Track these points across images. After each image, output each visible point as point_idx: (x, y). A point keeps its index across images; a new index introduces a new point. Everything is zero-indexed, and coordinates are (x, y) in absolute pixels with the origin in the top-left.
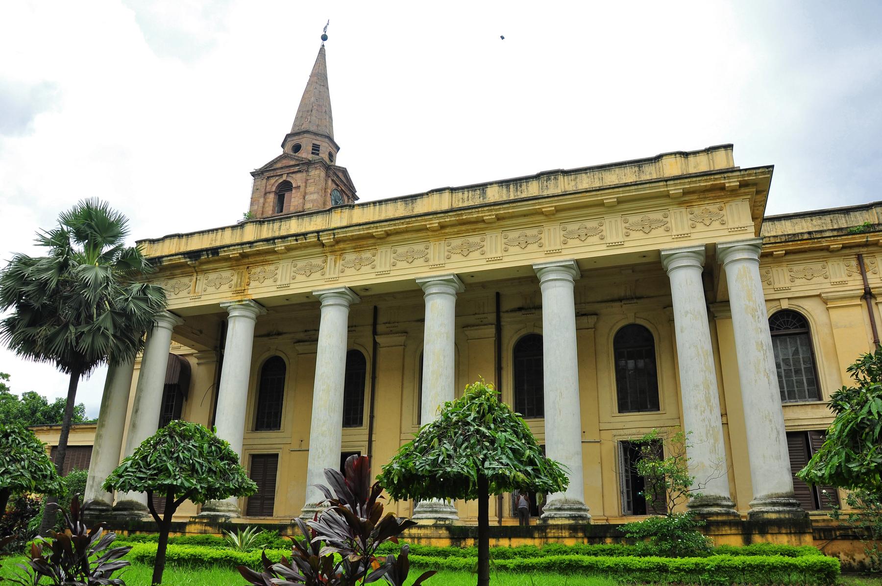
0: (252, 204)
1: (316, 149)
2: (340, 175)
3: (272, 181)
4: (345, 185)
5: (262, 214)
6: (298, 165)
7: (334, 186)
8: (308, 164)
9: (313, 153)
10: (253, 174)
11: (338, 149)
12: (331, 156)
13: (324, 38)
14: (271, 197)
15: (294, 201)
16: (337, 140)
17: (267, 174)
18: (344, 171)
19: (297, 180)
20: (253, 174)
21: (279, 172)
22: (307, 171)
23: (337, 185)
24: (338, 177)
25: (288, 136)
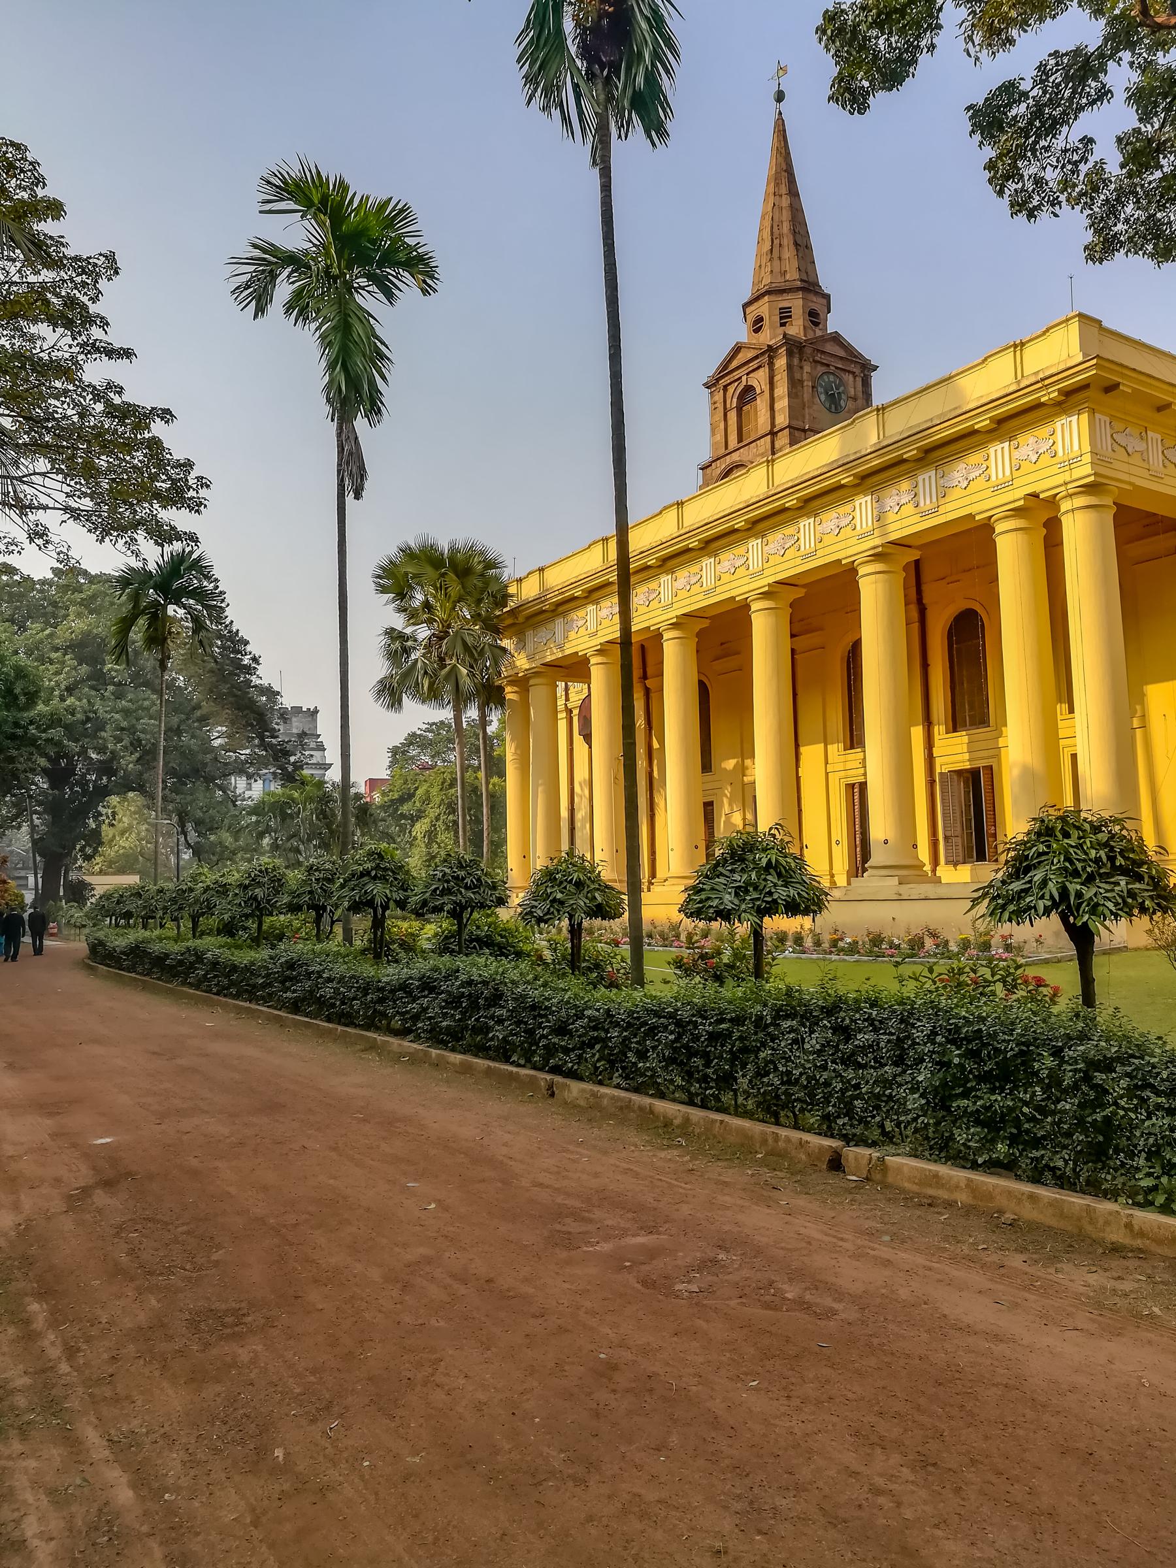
0: (713, 432)
1: (785, 316)
2: (830, 348)
3: (731, 389)
4: (841, 358)
5: (726, 448)
6: (756, 357)
7: (821, 369)
8: (771, 351)
9: (783, 325)
10: (708, 386)
11: (827, 297)
12: (815, 318)
13: (780, 97)
14: (733, 416)
15: (760, 417)
16: (826, 282)
17: (722, 382)
18: (836, 338)
19: (759, 380)
20: (708, 386)
21: (736, 375)
22: (771, 364)
23: (828, 365)
24: (823, 352)
25: (745, 306)
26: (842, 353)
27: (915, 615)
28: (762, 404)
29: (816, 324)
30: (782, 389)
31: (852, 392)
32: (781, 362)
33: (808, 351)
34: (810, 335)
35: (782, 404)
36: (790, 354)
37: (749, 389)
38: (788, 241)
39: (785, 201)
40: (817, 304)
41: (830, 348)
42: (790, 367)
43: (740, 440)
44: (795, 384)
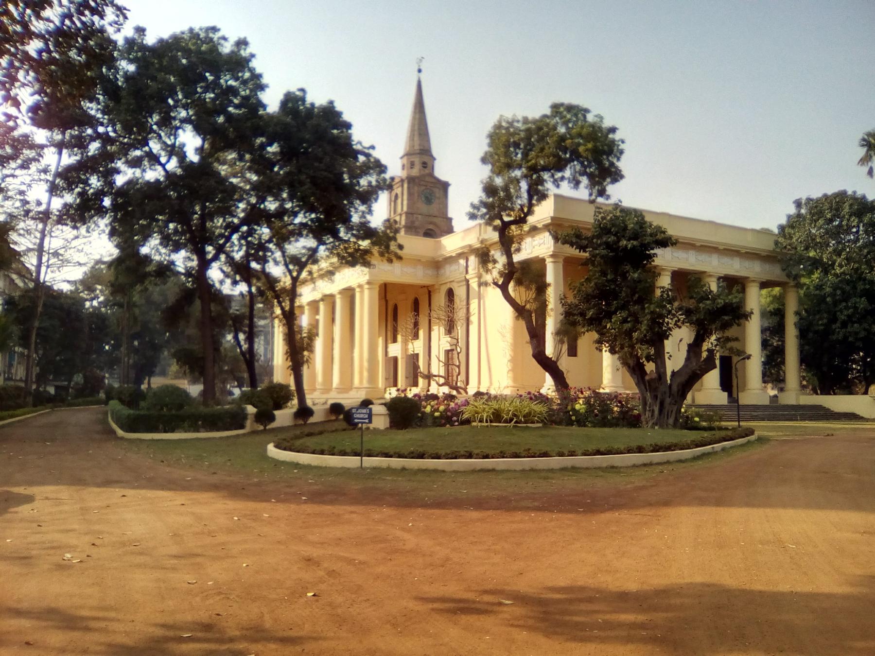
13: (420, 71)
14: (393, 204)
22: (402, 186)
26: (433, 180)
27: (384, 302)
28: (399, 201)
29: (425, 167)
30: (405, 197)
31: (437, 195)
32: (406, 186)
33: (417, 181)
34: (422, 172)
35: (405, 202)
36: (409, 183)
37: (396, 196)
38: (416, 133)
39: (417, 116)
40: (426, 159)
41: (427, 179)
42: (409, 188)
44: (410, 194)
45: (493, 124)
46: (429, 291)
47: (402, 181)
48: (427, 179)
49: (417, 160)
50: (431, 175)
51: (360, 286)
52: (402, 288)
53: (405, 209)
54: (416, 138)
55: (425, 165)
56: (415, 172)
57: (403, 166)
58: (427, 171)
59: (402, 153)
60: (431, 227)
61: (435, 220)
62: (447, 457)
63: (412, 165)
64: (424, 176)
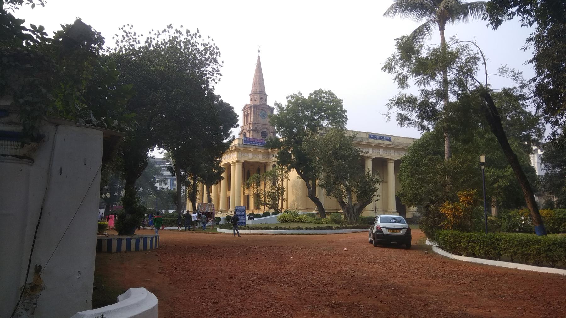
13: (259, 51)
28: (249, 116)
30: (252, 115)
35: (252, 118)
36: (254, 108)
38: (258, 83)
43: (247, 122)
45: (294, 90)
46: (265, 165)
47: (251, 107)
48: (263, 106)
49: (258, 96)
50: (265, 104)
51: (234, 163)
52: (252, 164)
53: (252, 121)
54: (258, 85)
55: (262, 99)
56: (257, 103)
57: (251, 99)
58: (263, 102)
59: (250, 93)
60: (265, 130)
61: (267, 126)
62: (274, 229)
63: (256, 99)
64: (261, 105)
